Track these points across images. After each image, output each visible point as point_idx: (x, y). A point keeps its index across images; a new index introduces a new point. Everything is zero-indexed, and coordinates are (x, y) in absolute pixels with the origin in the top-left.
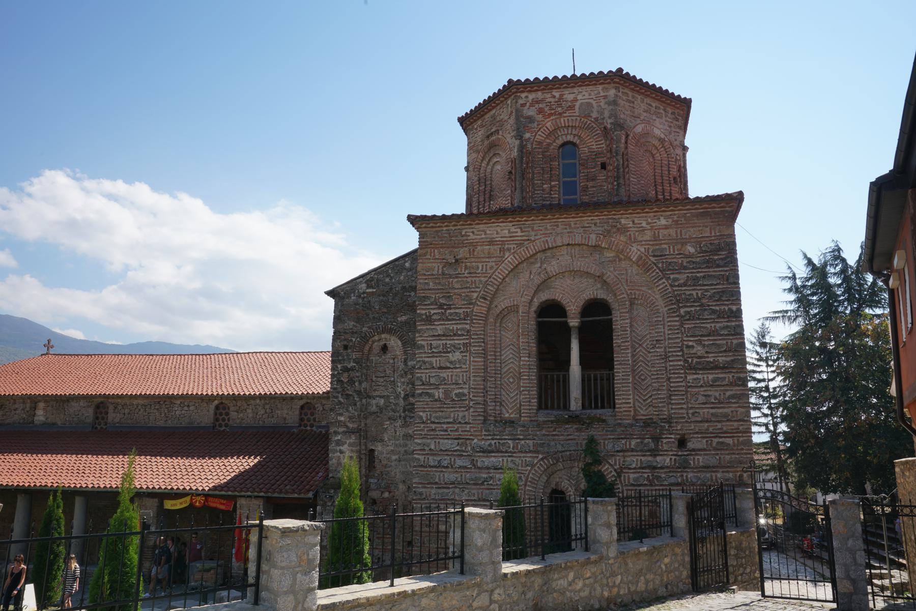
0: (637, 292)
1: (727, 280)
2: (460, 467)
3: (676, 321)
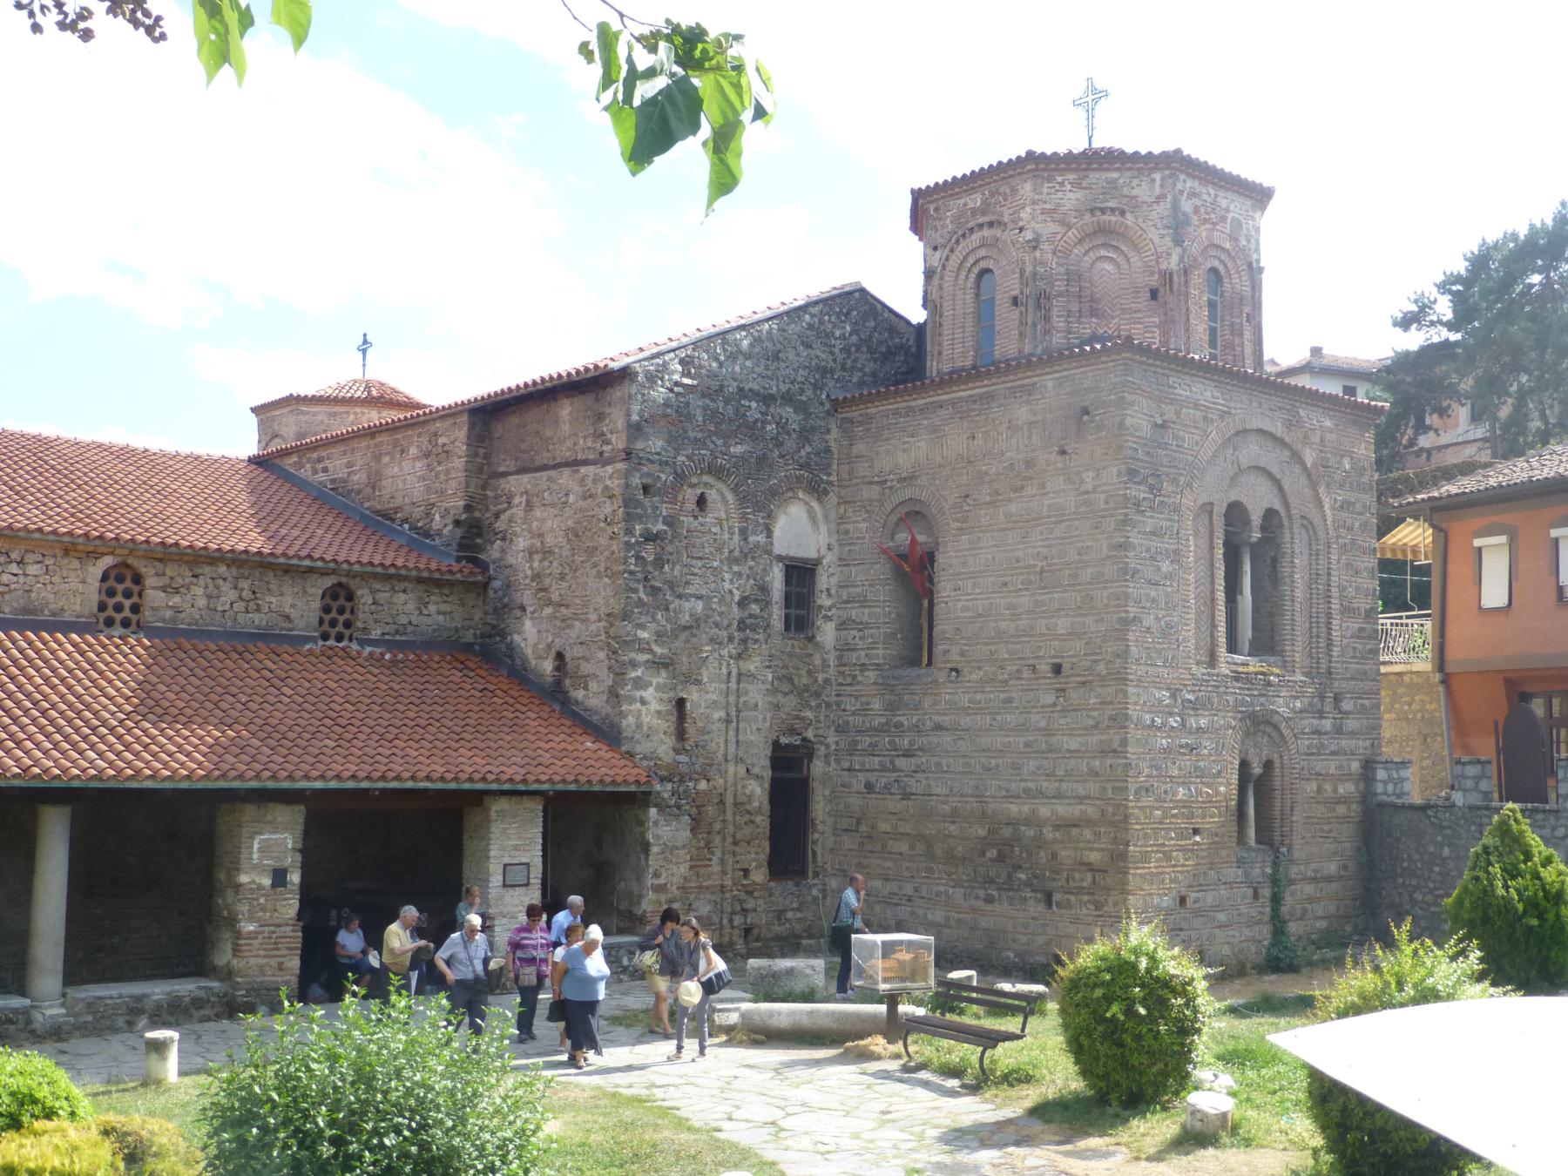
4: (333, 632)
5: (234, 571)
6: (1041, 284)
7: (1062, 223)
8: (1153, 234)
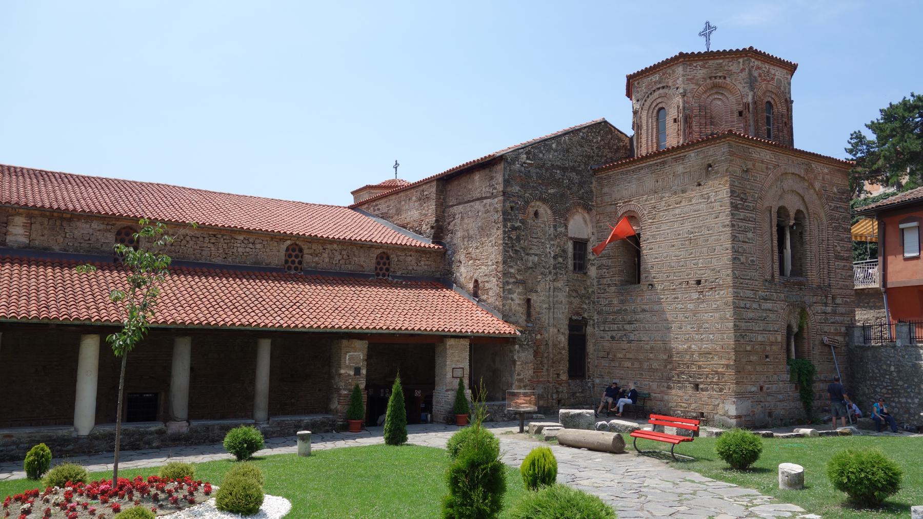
2: (755, 309)
4: (381, 273)
6: (687, 112)
7: (697, 84)
8: (740, 87)
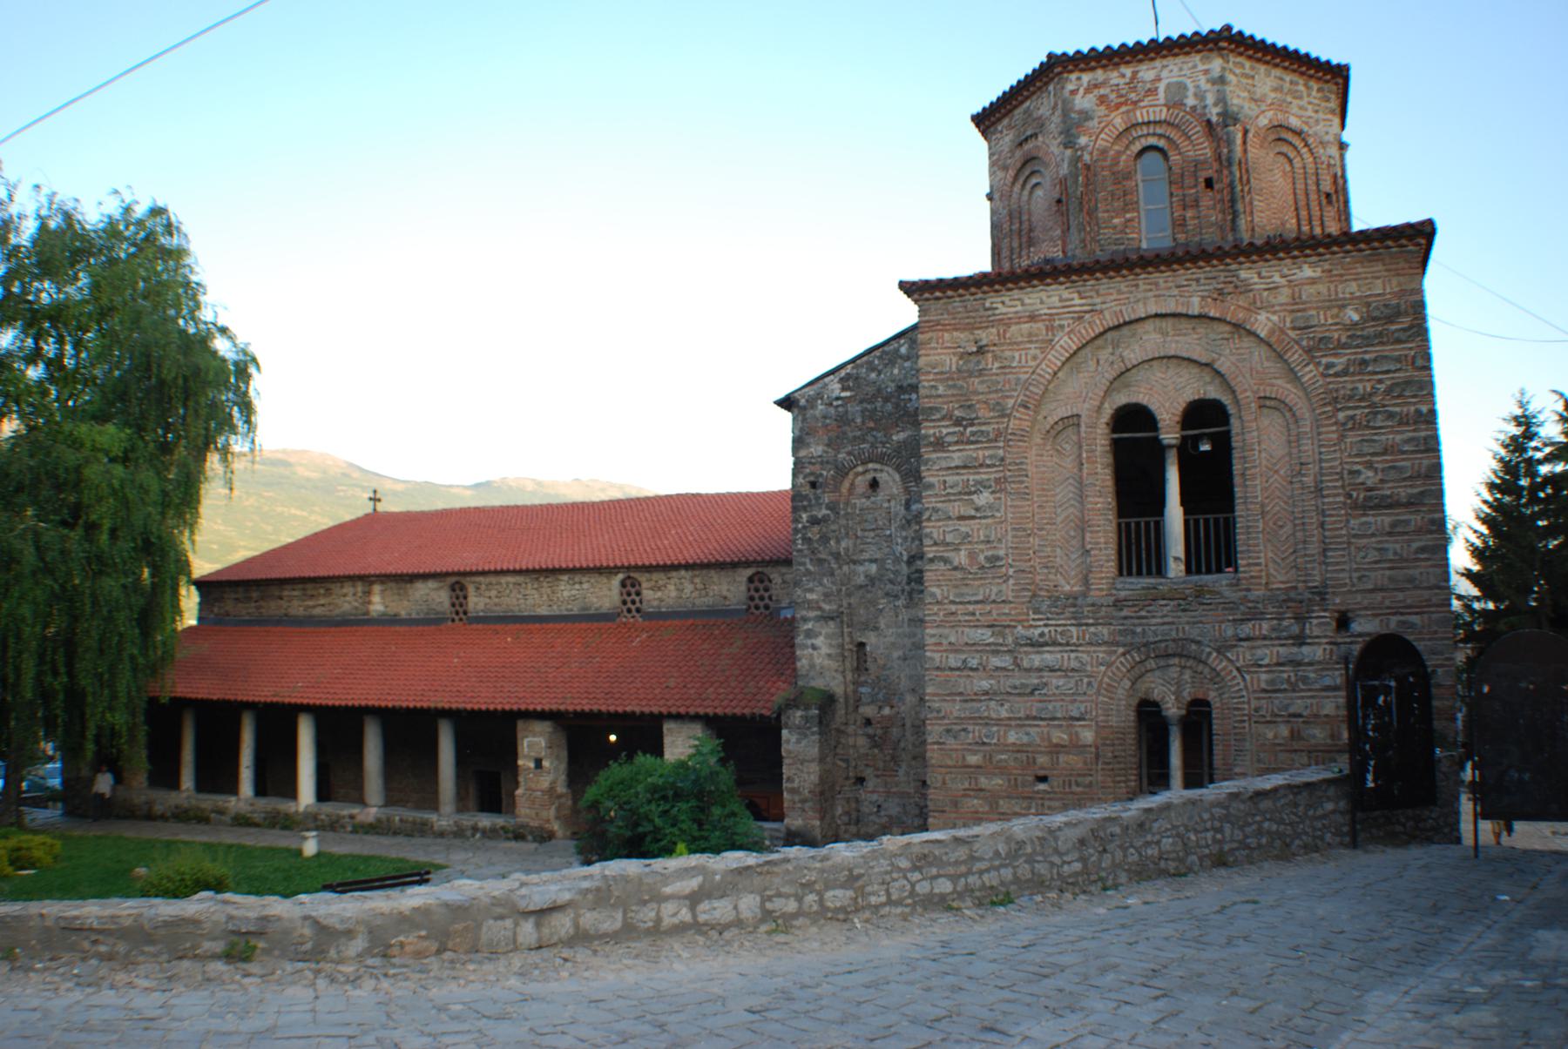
0: (1268, 388)
1: (1413, 363)
2: (997, 668)
3: (1333, 432)
5: (690, 573)
